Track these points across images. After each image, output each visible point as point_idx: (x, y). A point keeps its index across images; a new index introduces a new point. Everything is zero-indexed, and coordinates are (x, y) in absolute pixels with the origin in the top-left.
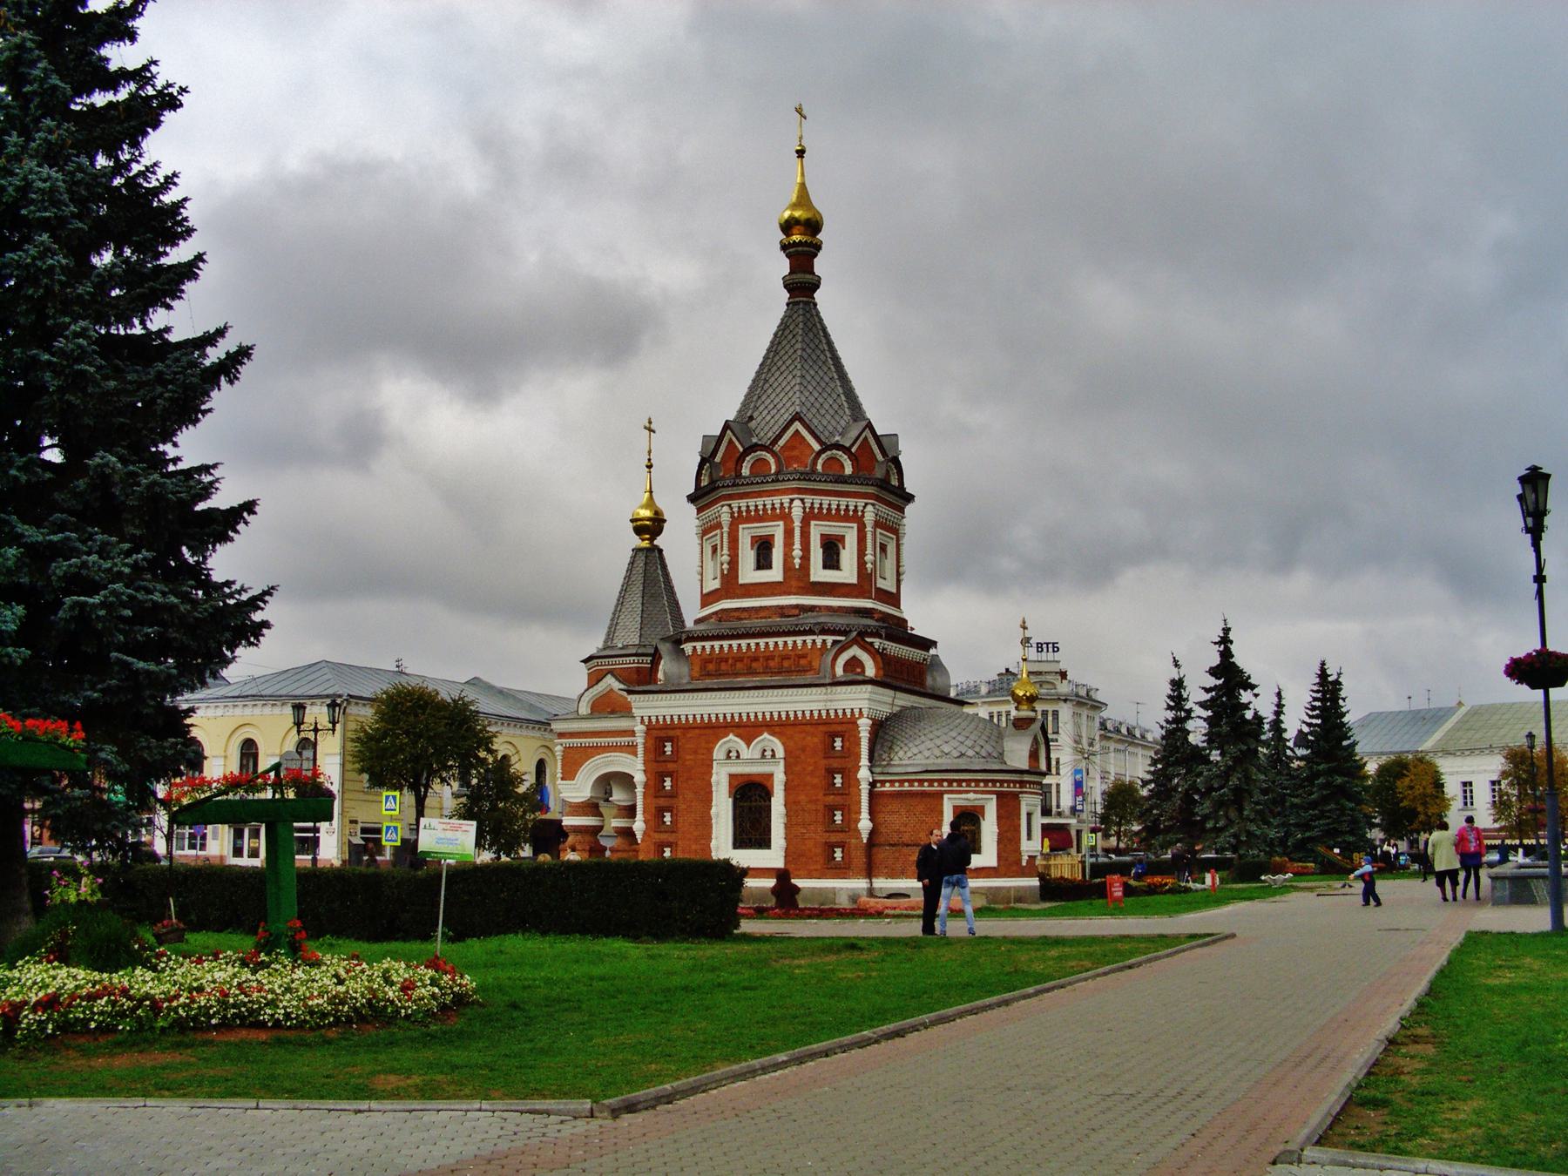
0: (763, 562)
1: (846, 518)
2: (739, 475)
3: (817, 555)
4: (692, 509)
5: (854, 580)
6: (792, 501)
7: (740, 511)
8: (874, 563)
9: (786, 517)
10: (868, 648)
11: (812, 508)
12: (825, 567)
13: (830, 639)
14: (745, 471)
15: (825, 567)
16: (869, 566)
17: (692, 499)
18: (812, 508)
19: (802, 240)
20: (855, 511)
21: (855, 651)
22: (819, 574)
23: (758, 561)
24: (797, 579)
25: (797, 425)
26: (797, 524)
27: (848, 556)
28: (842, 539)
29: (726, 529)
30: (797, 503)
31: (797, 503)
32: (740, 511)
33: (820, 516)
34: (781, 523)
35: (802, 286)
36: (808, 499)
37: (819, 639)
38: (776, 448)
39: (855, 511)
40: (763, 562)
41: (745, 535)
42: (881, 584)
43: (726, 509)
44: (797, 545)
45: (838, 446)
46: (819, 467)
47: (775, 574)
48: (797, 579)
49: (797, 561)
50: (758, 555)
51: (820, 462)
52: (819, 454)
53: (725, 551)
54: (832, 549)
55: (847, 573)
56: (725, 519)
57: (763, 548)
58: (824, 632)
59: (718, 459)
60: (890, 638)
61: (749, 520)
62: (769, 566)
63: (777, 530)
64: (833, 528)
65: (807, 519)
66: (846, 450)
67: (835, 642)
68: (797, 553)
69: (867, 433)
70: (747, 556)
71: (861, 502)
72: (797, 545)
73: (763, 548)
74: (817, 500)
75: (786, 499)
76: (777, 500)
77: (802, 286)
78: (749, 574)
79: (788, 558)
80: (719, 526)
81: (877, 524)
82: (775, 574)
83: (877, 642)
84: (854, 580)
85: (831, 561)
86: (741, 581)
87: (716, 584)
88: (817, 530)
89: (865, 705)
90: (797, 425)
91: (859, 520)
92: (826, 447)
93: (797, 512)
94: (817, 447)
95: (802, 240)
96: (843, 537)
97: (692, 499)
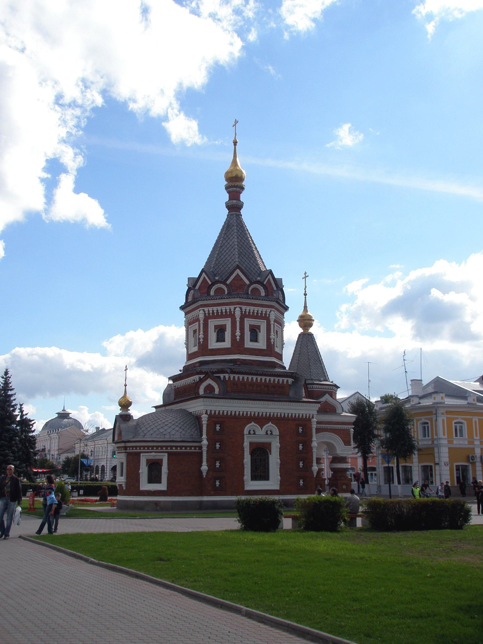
0: (220, 338)
2: (209, 294)
4: (182, 313)
5: (265, 348)
6: (235, 308)
7: (209, 314)
11: (245, 312)
12: (251, 341)
14: (212, 293)
15: (251, 341)
16: (272, 340)
17: (182, 308)
18: (245, 312)
19: (235, 183)
20: (266, 314)
22: (248, 344)
24: (238, 347)
25: (238, 271)
26: (238, 319)
27: (262, 335)
28: (259, 327)
29: (202, 322)
30: (238, 309)
31: (238, 309)
32: (209, 314)
33: (249, 316)
34: (230, 319)
35: (234, 207)
36: (244, 308)
38: (228, 282)
39: (266, 314)
40: (220, 338)
41: (212, 324)
43: (202, 312)
44: (238, 330)
47: (227, 344)
48: (238, 347)
49: (238, 338)
50: (218, 335)
51: (250, 289)
52: (249, 286)
53: (201, 332)
54: (254, 331)
56: (202, 316)
57: (221, 330)
59: (197, 287)
62: (224, 341)
63: (228, 322)
68: (238, 333)
69: (270, 276)
70: (212, 335)
71: (268, 310)
72: (238, 330)
73: (221, 330)
74: (248, 308)
75: (232, 307)
76: (228, 308)
77: (234, 207)
78: (213, 344)
80: (198, 320)
81: (275, 321)
82: (227, 344)
84: (265, 348)
85: (254, 338)
86: (209, 348)
87: (196, 349)
88: (248, 322)
90: (238, 271)
91: (267, 318)
93: (238, 314)
94: (247, 282)
95: (235, 183)
96: (260, 326)
97: (182, 308)
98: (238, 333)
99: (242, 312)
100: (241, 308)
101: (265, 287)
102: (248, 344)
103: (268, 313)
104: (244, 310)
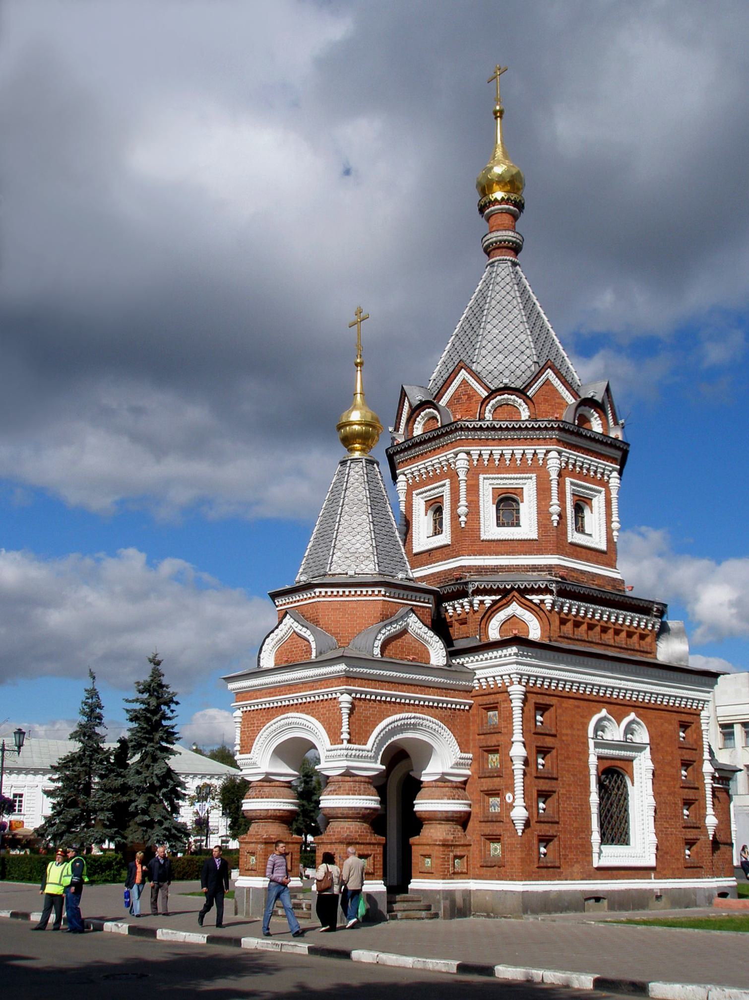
1: (523, 468)
3: (488, 510)
8: (562, 516)
9: (453, 475)
10: (537, 609)
13: (488, 600)
21: (514, 609)
23: (435, 528)
24: (466, 538)
27: (528, 509)
31: (462, 456)
36: (475, 451)
37: (477, 600)
38: (443, 402)
42: (574, 537)
44: (463, 502)
45: (506, 389)
46: (488, 416)
54: (507, 503)
55: (528, 527)
58: (478, 592)
60: (562, 593)
61: (423, 484)
64: (508, 481)
65: (473, 473)
66: (521, 392)
67: (495, 602)
68: (462, 510)
71: (541, 450)
72: (463, 502)
75: (450, 454)
79: (455, 517)
83: (548, 599)
84: (535, 536)
89: (513, 668)
92: (493, 393)
98: (462, 510)
99: (470, 461)
100: (468, 453)
101: (528, 400)
102: (490, 530)
103: (541, 456)
104: (475, 457)
